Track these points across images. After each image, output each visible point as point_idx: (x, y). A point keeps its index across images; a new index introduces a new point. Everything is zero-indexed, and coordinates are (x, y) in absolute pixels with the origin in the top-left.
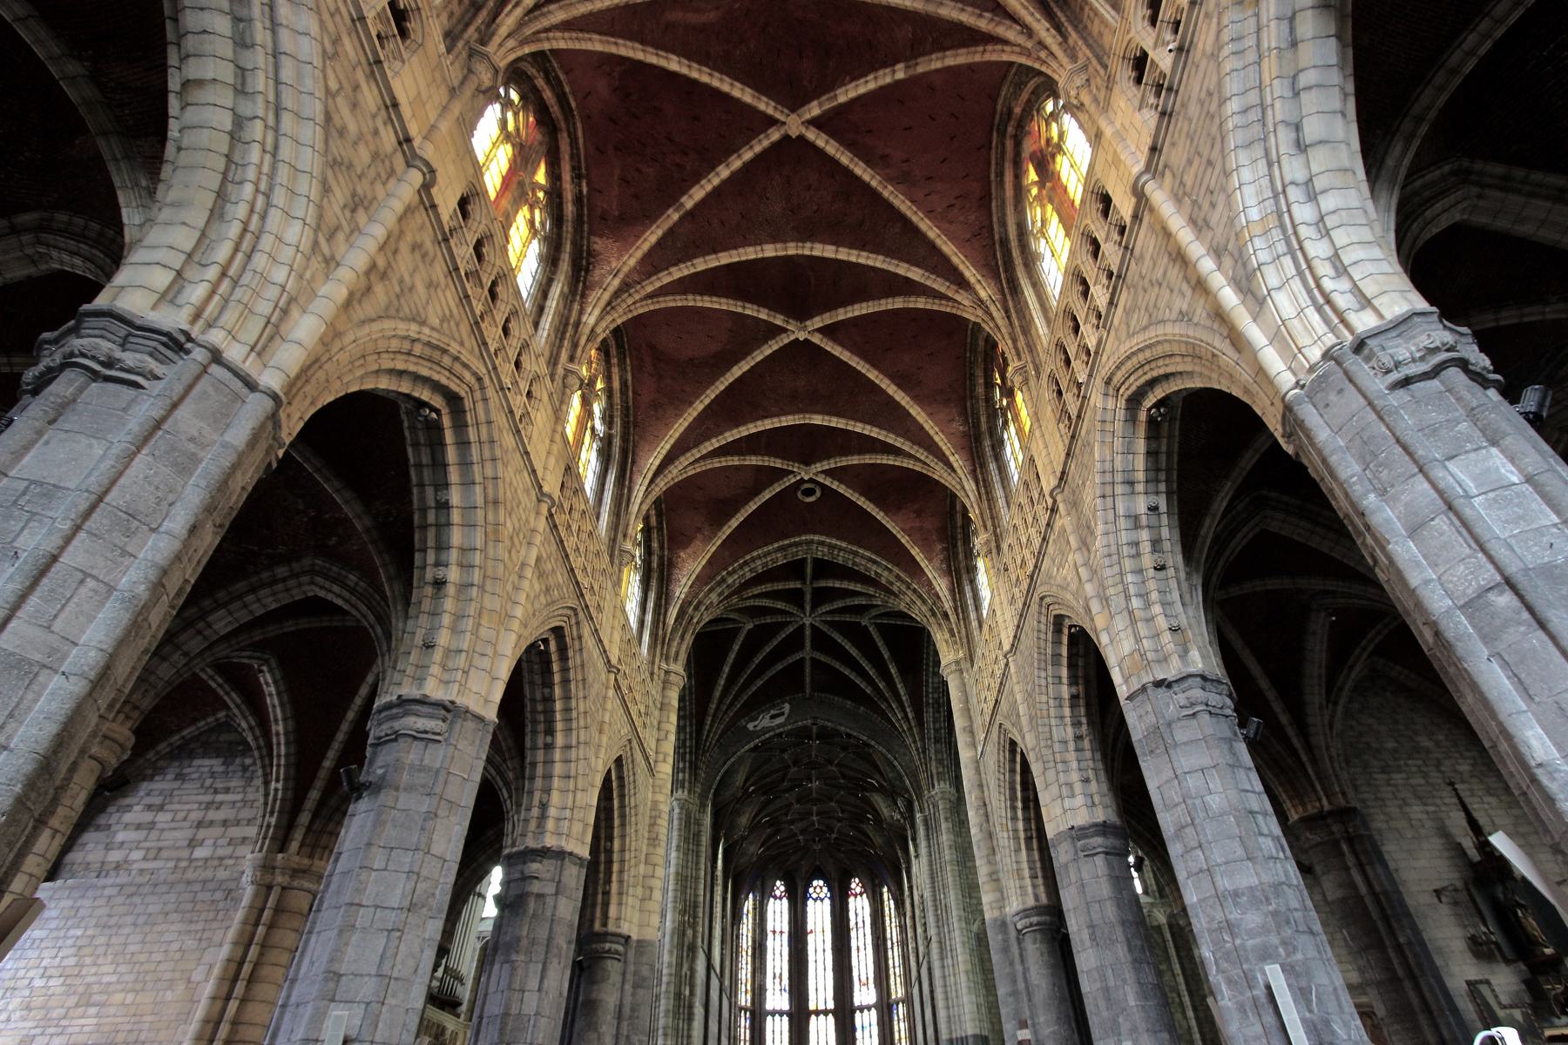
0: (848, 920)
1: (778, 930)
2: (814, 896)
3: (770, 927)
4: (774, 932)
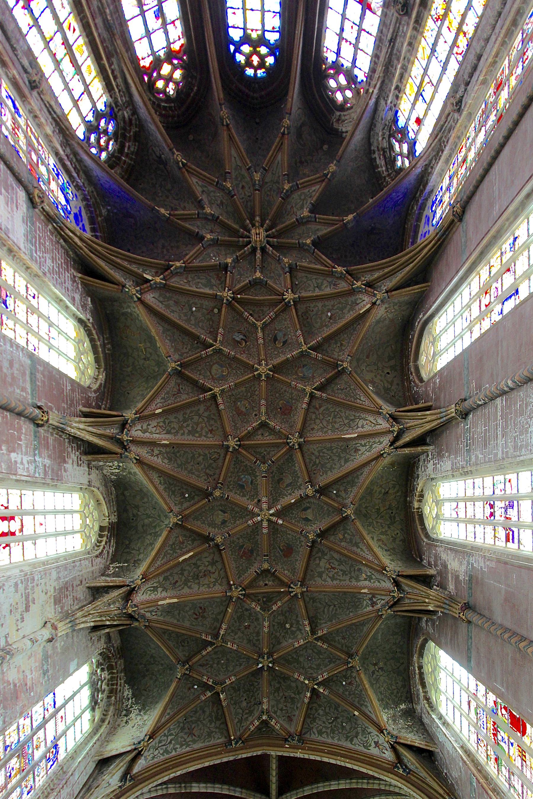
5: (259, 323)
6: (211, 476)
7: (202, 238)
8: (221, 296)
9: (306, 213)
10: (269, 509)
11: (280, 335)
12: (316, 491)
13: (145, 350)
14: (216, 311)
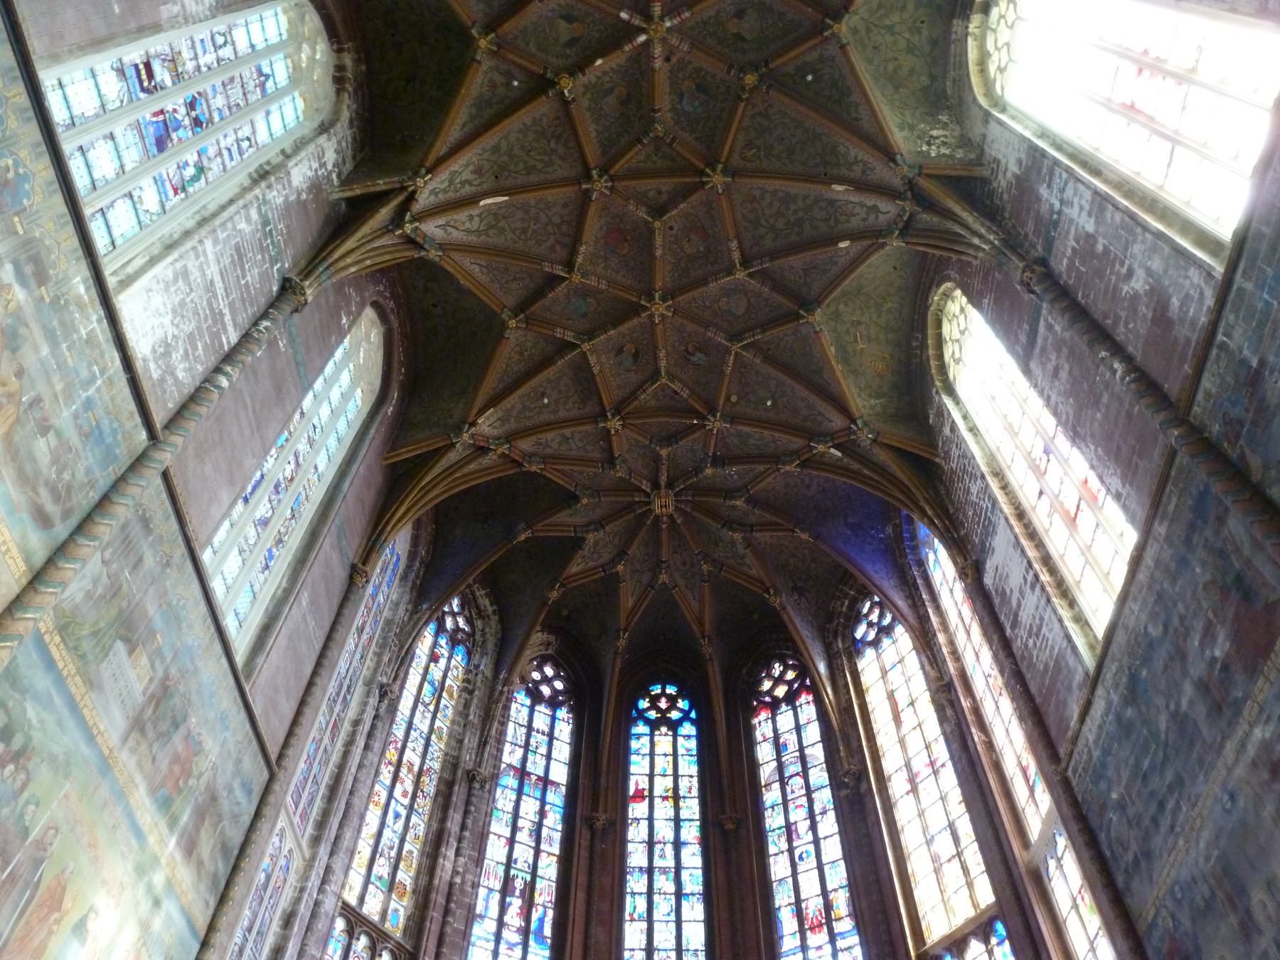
0: (754, 766)
1: (536, 766)
2: (652, 715)
3: (511, 756)
4: (522, 773)
5: (664, 381)
6: (760, 114)
7: (748, 501)
8: (725, 422)
9: (591, 538)
10: (647, 43)
11: (628, 361)
12: (552, 84)
13: (856, 337)
14: (734, 399)
